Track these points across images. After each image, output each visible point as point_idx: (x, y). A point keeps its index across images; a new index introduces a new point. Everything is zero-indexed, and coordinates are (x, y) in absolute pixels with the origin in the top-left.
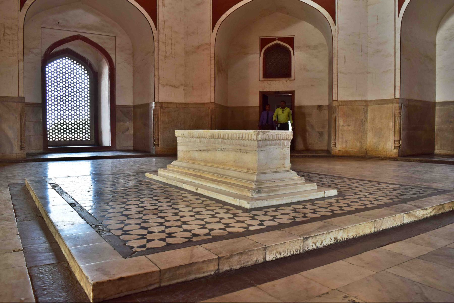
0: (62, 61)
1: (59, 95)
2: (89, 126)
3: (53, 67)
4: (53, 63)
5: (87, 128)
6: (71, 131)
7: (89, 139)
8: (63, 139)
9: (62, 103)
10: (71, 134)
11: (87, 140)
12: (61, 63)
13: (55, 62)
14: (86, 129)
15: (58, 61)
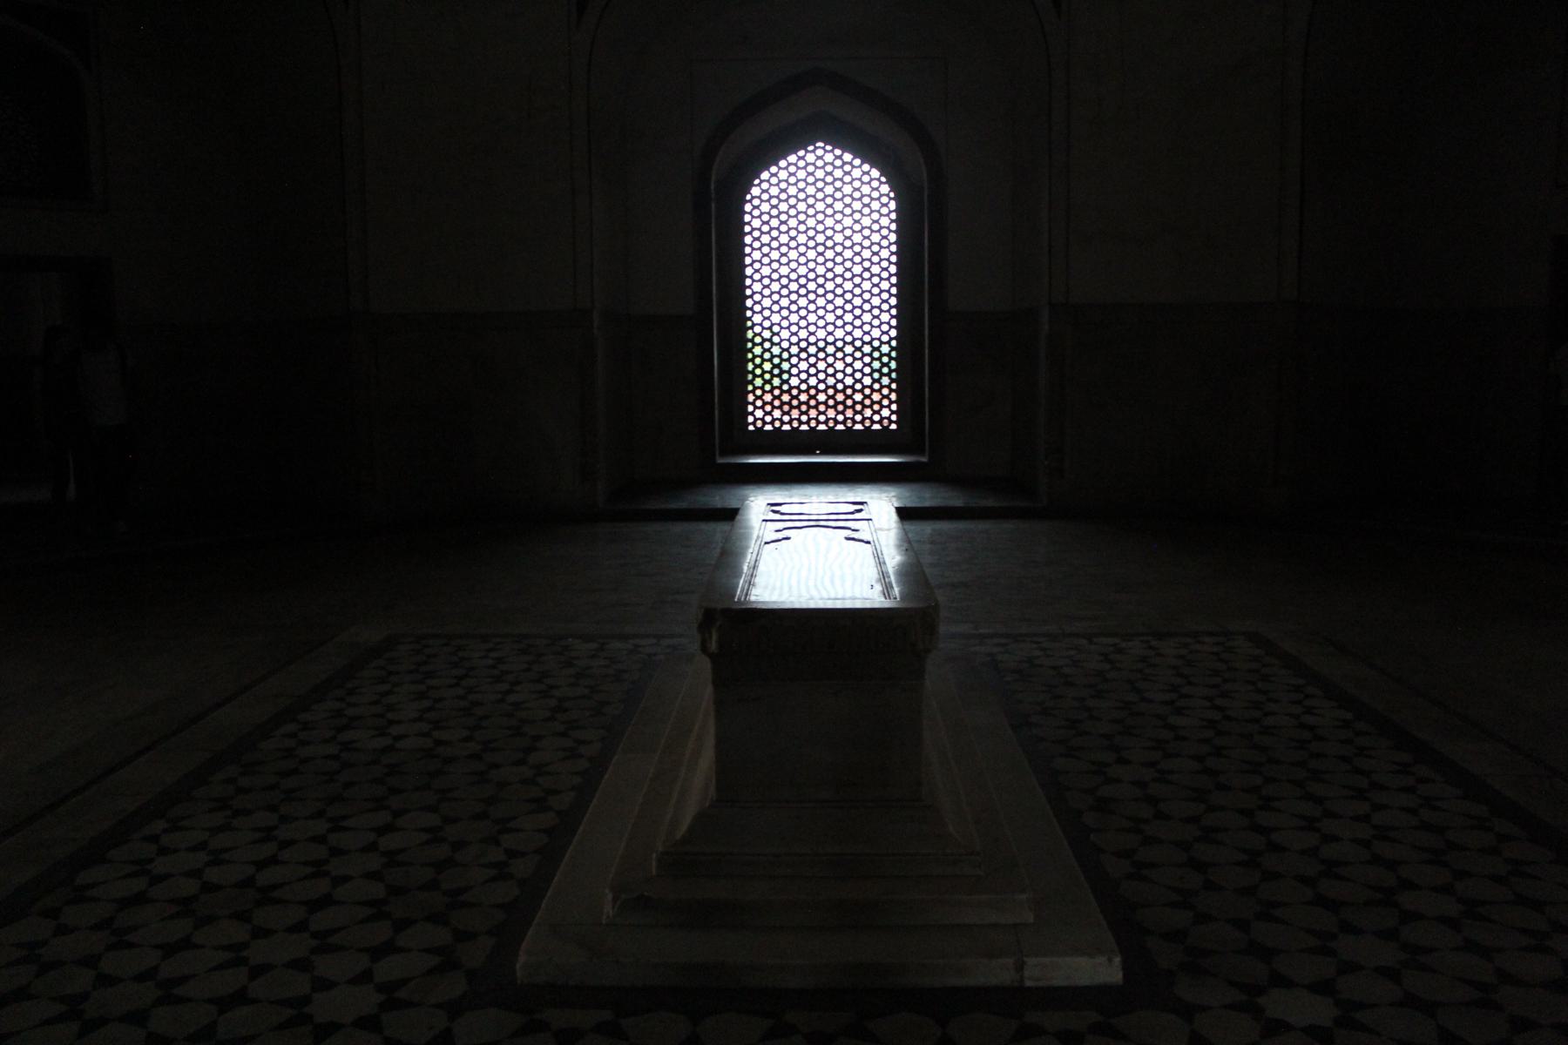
0: (802, 158)
1: (793, 276)
2: (892, 381)
3: (774, 180)
4: (774, 169)
5: (888, 386)
6: (832, 397)
7: (894, 426)
8: (808, 423)
9: (803, 302)
10: (835, 407)
11: (886, 429)
12: (801, 164)
13: (783, 163)
14: (885, 391)
15: (792, 158)
